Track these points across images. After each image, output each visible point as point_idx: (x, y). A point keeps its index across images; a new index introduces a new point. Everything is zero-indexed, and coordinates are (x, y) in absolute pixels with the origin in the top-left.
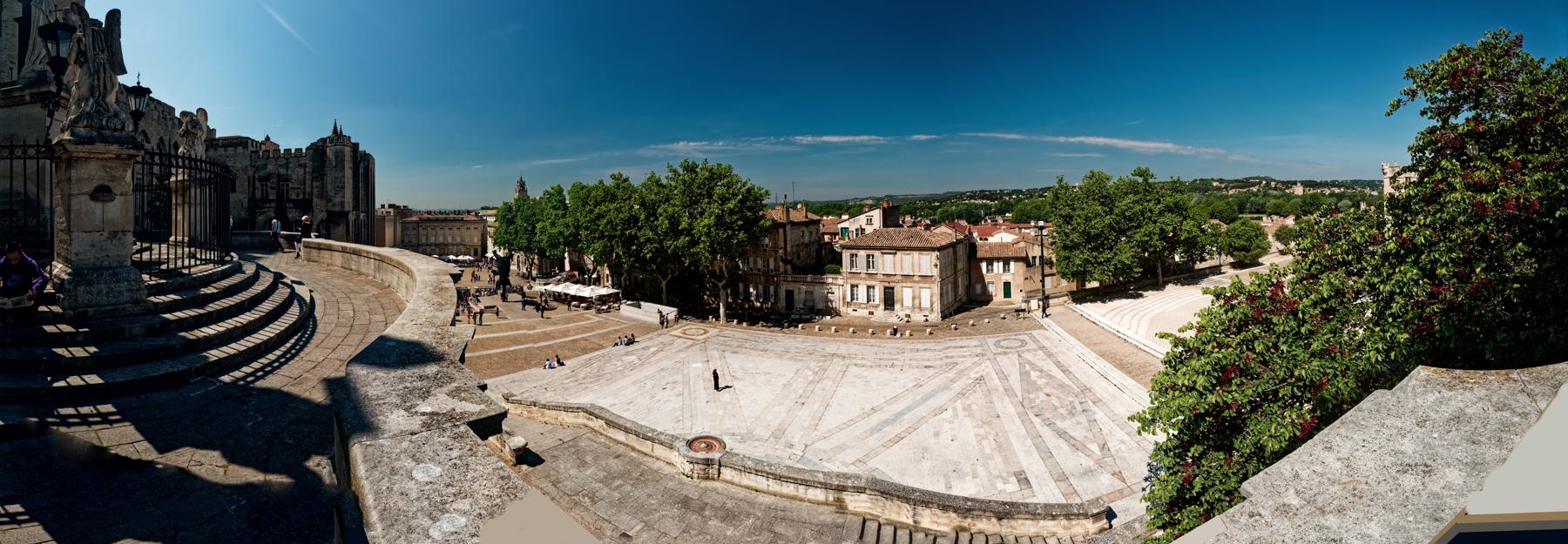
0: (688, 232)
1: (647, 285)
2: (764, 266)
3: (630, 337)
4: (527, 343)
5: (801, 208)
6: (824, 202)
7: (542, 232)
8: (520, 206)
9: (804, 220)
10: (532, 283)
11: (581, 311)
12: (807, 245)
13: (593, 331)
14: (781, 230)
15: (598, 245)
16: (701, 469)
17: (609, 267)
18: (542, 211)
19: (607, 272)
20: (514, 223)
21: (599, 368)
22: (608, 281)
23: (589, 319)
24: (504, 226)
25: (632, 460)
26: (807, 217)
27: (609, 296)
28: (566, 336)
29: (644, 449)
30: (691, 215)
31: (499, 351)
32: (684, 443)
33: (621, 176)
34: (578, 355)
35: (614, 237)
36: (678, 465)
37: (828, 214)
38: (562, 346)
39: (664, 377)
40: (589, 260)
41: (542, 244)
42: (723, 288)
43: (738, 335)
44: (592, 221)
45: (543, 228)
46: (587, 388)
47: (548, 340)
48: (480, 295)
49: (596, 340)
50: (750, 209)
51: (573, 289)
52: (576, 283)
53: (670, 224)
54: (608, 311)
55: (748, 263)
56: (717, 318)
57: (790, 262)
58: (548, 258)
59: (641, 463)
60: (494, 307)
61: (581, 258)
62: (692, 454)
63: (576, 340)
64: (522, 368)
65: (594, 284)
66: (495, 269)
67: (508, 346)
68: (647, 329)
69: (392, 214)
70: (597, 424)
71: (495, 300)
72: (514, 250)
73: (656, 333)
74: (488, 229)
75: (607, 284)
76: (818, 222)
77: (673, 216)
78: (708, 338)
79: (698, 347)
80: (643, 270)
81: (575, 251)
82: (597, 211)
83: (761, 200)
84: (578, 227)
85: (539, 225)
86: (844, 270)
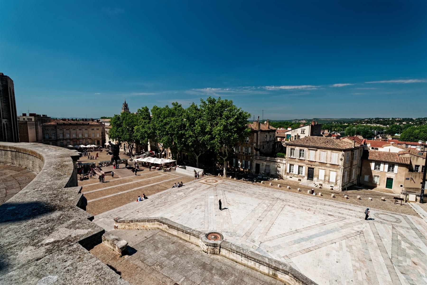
0: (210, 133)
1: (189, 158)
2: (246, 151)
3: (180, 183)
4: (128, 189)
5: (266, 124)
6: (278, 121)
7: (137, 131)
8: (124, 117)
9: (267, 129)
10: (132, 158)
11: (156, 171)
12: (268, 142)
13: (162, 180)
14: (255, 134)
15: (165, 138)
16: (212, 249)
17: (171, 149)
18: (137, 120)
19: (170, 151)
20: (121, 126)
21: (165, 199)
22: (170, 156)
23: (160, 175)
24: (115, 128)
25: (180, 244)
26: (269, 128)
27: (171, 163)
28: (148, 184)
29: (186, 239)
30: (212, 125)
31: (111, 195)
32: (204, 235)
33: (177, 104)
34: (155, 193)
35: (173, 134)
36: (201, 247)
37: (280, 127)
38: (146, 189)
39: (196, 203)
40: (160, 146)
41: (137, 138)
42: (225, 160)
43: (231, 183)
44: (162, 126)
45: (138, 129)
46: (159, 209)
47: (139, 186)
48: (102, 167)
49: (164, 185)
50: (240, 123)
51: (152, 160)
52: (154, 157)
53: (201, 128)
54: (170, 171)
55: (238, 149)
56: (222, 175)
57: (259, 150)
58: (141, 144)
59: (184, 246)
60: (111, 172)
61: (156, 144)
62: (208, 241)
63: (154, 186)
64: (125, 203)
65: (163, 157)
66: (110, 151)
67: (117, 192)
68: (189, 179)
69: (33, 120)
70: (164, 227)
71: (111, 168)
72: (121, 141)
73: (193, 181)
74: (106, 129)
75: (169, 157)
76: (275, 131)
77: (202, 125)
78: (217, 184)
79: (212, 188)
80: (187, 151)
81: (153, 141)
82: (165, 121)
83: (246, 119)
84: (155, 129)
85: (136, 128)
86: (287, 156)
